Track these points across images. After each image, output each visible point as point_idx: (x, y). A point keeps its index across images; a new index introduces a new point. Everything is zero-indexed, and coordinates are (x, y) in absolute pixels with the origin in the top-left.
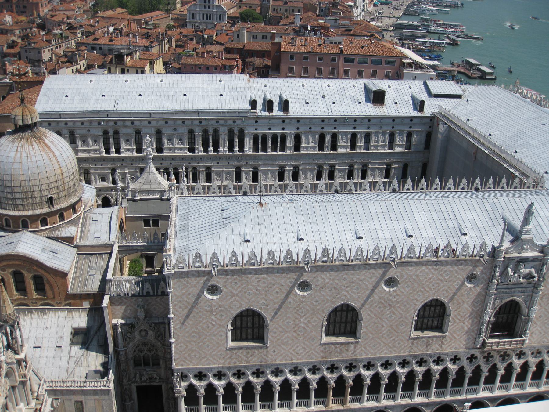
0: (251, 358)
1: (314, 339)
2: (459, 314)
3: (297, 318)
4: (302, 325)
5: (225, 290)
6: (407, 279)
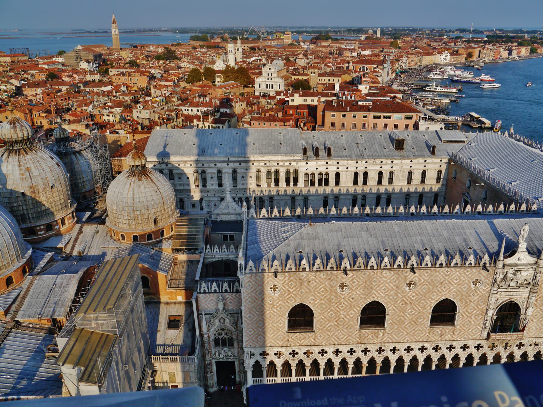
1: (350, 328)
2: (467, 311)
3: (338, 311)
4: (342, 316)
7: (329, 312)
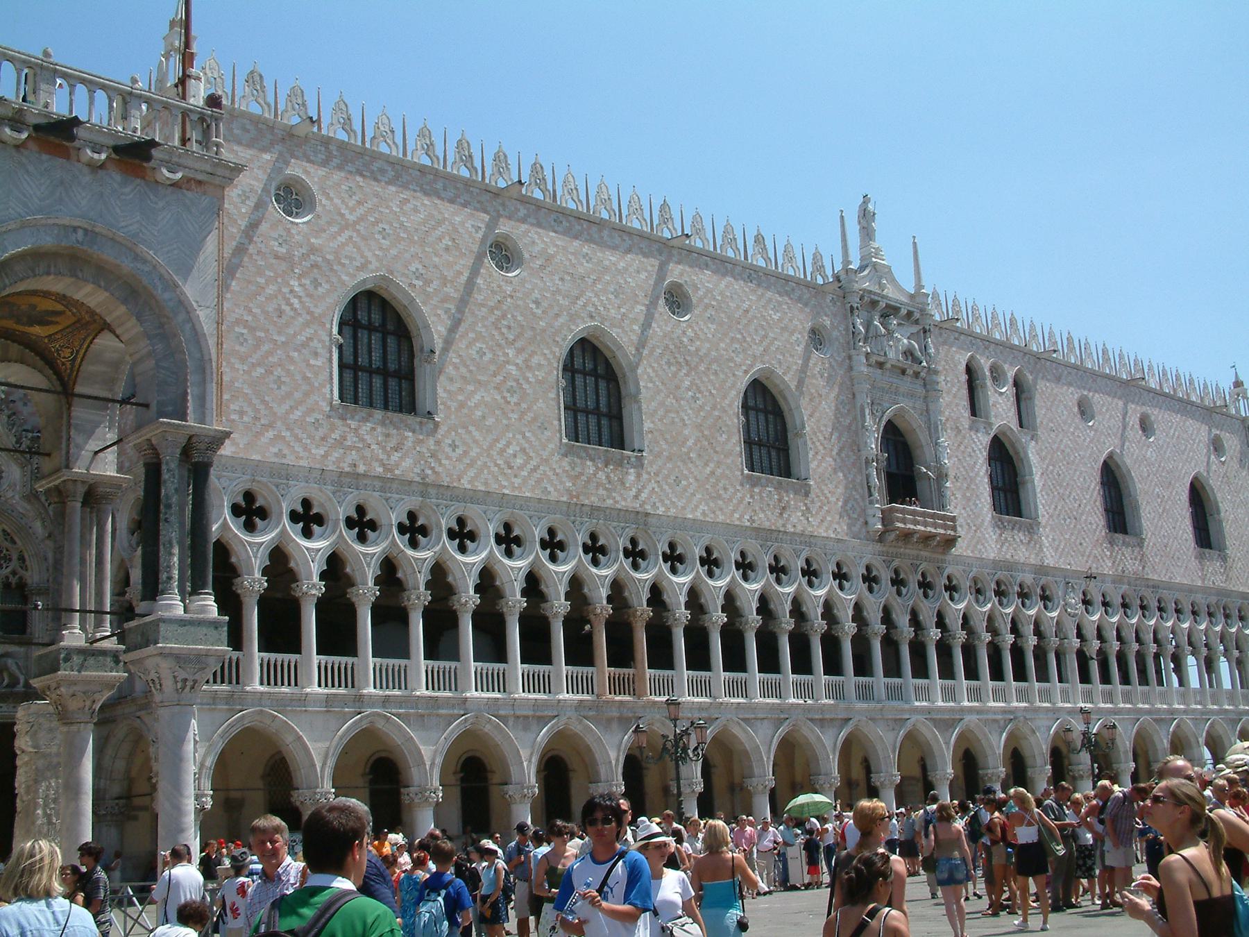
0: (396, 456)
1: (543, 428)
2: (818, 428)
3: (499, 345)
5: (324, 201)
6: (705, 296)
7: (475, 340)
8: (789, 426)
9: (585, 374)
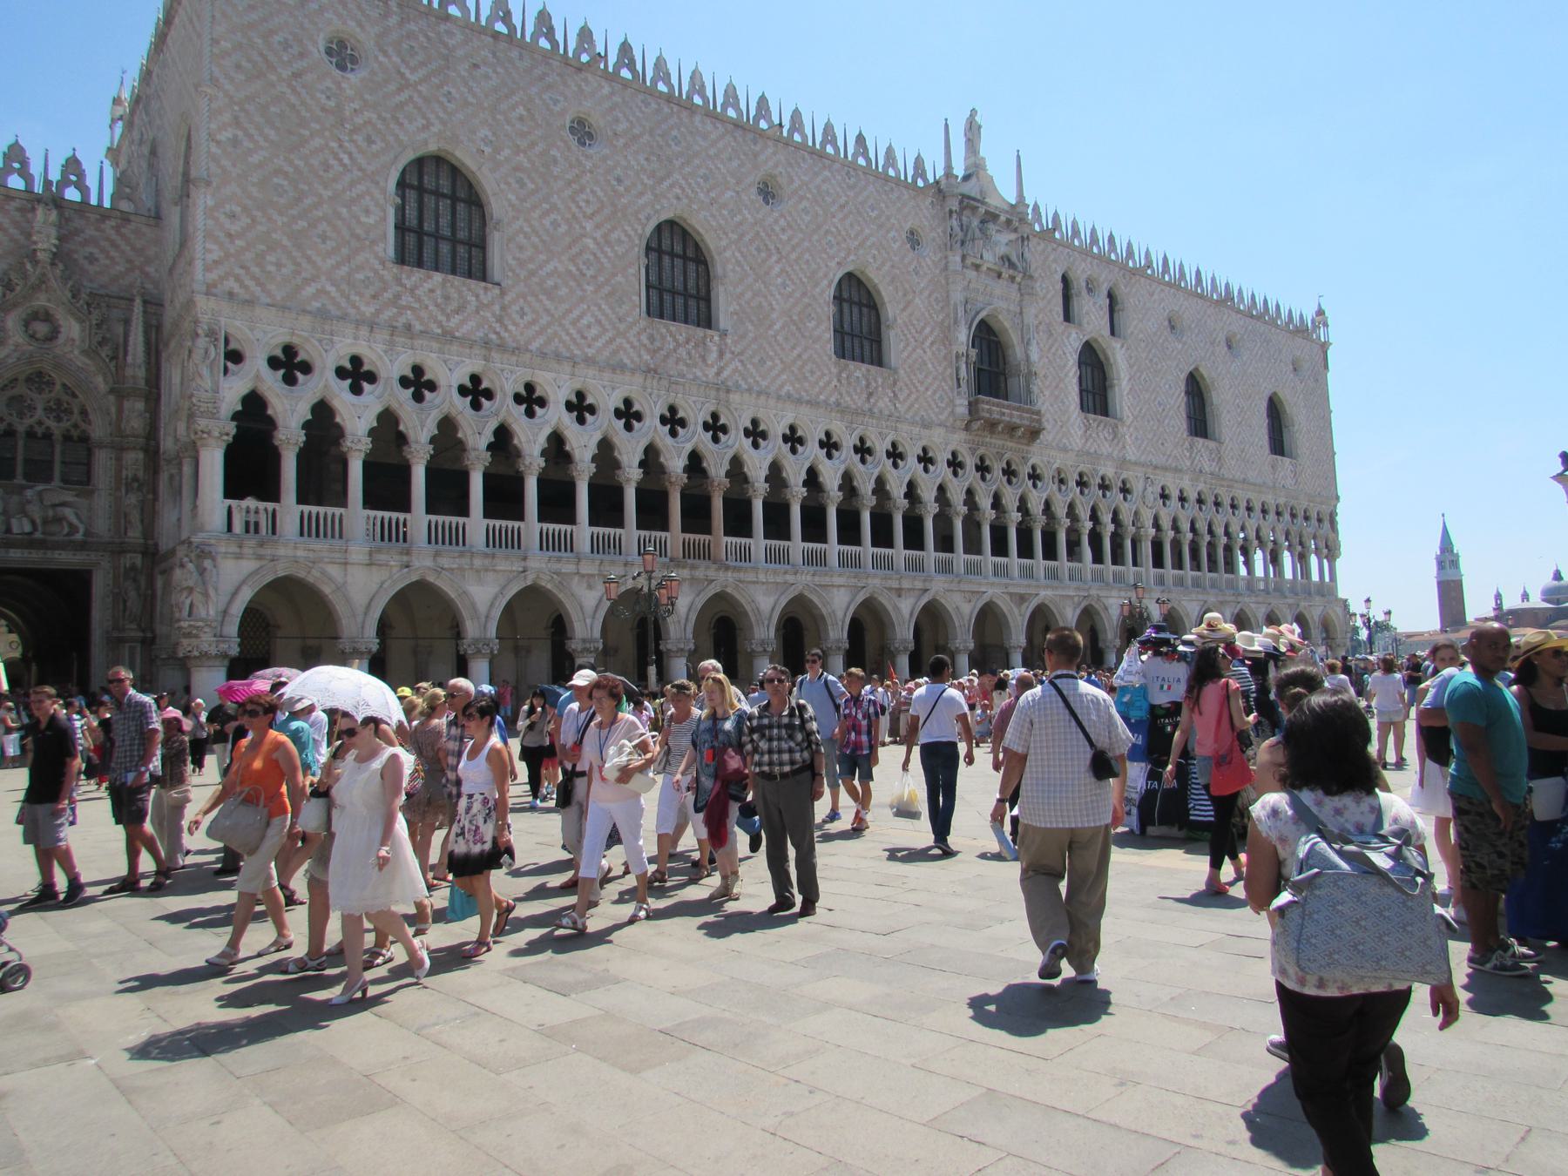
0: (456, 320)
3: (574, 215)
5: (381, 58)
8: (883, 319)
9: (672, 255)
